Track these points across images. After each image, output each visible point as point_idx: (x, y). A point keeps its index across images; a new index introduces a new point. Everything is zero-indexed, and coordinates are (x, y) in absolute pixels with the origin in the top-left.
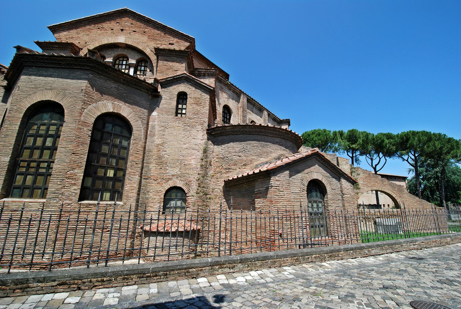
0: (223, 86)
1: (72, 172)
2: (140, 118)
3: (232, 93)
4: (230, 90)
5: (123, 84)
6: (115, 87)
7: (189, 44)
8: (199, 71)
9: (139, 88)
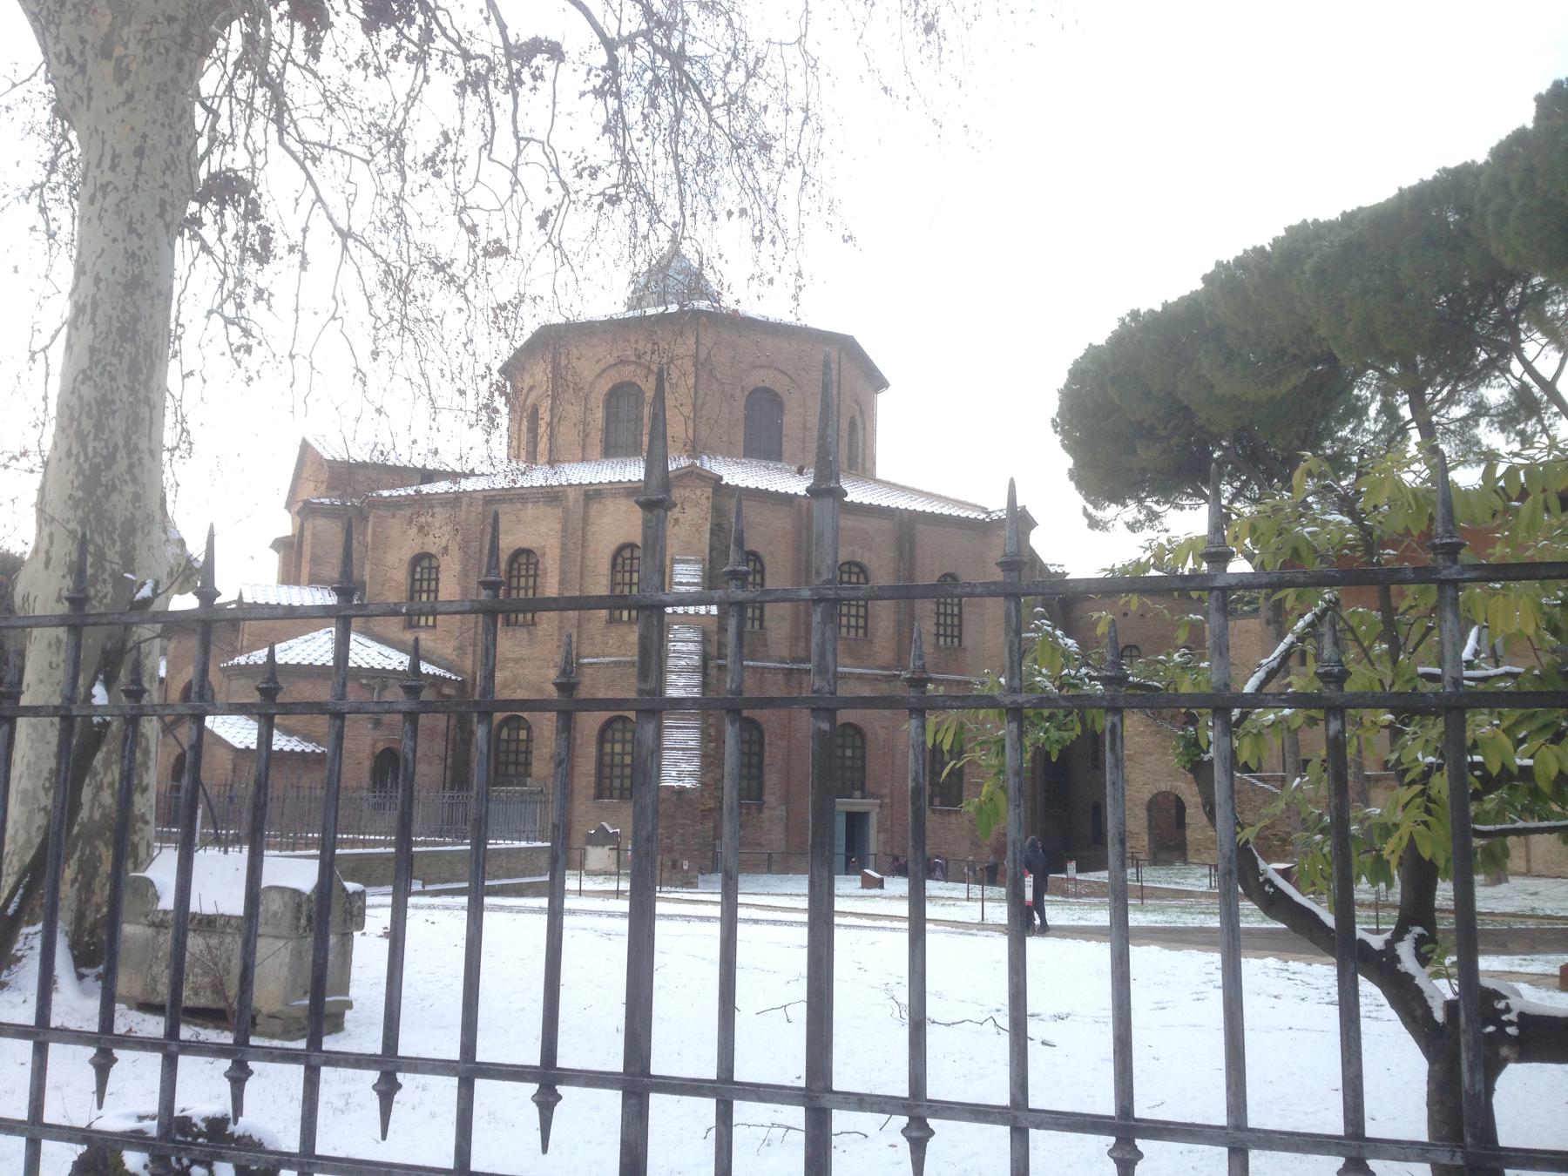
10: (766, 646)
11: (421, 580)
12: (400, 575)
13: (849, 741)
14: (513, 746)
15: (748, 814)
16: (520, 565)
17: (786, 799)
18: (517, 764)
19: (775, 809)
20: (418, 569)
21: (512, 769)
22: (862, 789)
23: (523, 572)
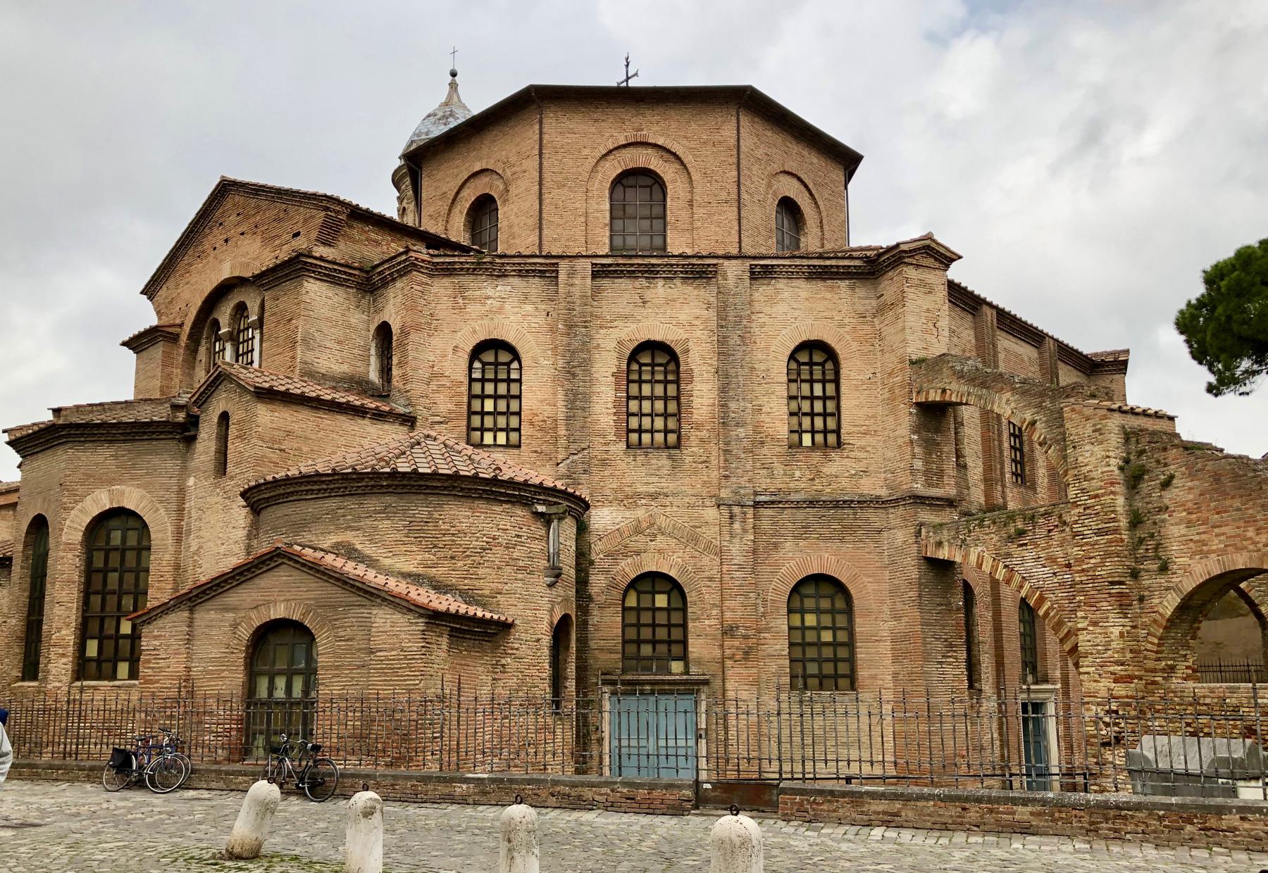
0: (466, 280)
1: (58, 634)
2: (161, 502)
3: (516, 281)
4: (504, 275)
5: (124, 441)
6: (112, 456)
7: (324, 213)
8: (379, 273)
9: (154, 436)
11: (483, 380)
12: (456, 368)
14: (646, 618)
16: (641, 365)
18: (654, 642)
20: (477, 365)
21: (646, 650)
23: (646, 377)
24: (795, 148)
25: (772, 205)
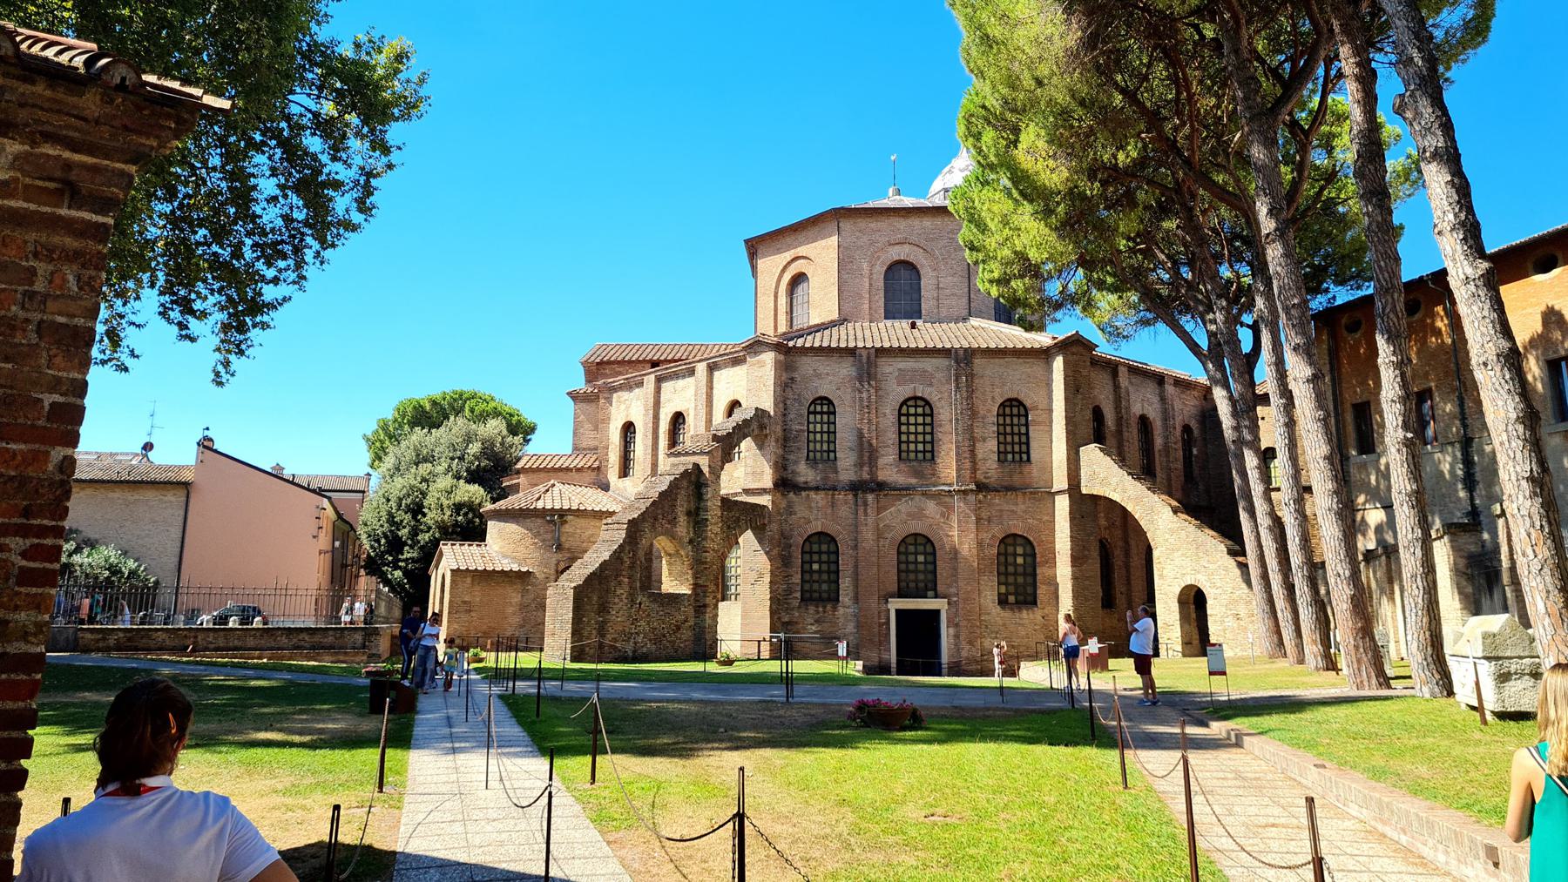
10: (837, 472)
13: (921, 548)
15: (824, 612)
17: (856, 599)
19: (848, 607)
22: (935, 590)
24: (901, 224)
25: (880, 270)
